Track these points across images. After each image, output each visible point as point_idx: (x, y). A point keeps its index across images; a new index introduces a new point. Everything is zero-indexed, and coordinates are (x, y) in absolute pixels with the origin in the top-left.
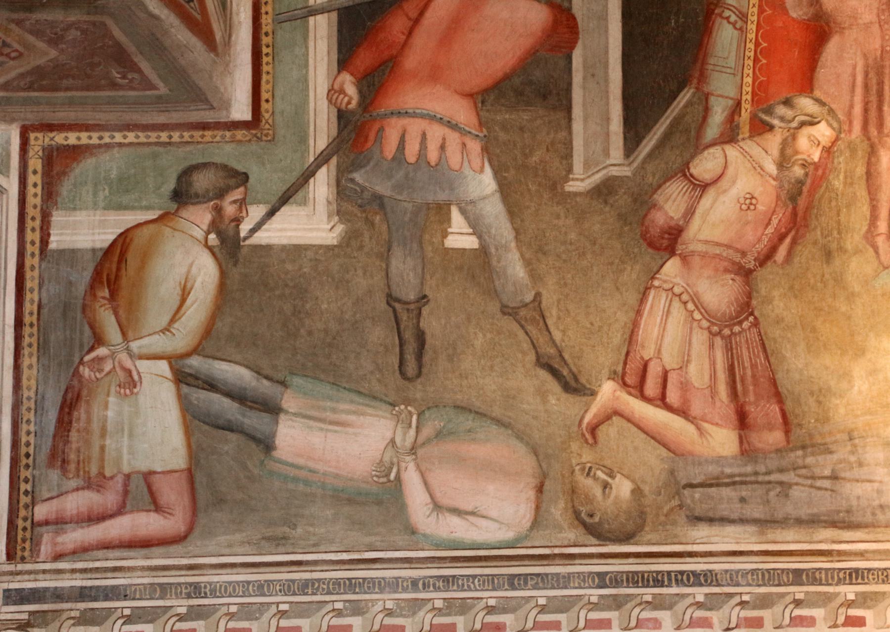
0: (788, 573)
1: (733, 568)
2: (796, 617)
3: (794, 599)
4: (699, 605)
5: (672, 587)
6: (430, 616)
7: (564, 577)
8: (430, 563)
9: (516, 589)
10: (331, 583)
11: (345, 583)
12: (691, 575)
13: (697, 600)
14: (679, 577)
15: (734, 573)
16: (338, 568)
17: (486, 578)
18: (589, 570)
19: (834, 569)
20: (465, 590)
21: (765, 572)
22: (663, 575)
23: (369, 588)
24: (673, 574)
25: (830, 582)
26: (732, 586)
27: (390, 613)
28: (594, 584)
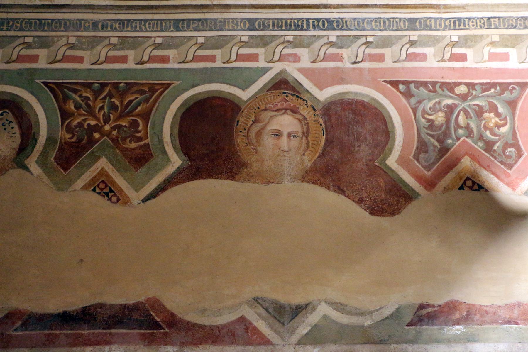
0: (404, 21)
1: (360, 17)
2: (411, 54)
3: (409, 40)
4: (332, 44)
5: (310, 30)
6: (106, 50)
7: (220, 22)
8: (110, 10)
9: (180, 31)
10: (24, 23)
11: (35, 22)
12: (326, 22)
13: (330, 40)
14: (316, 23)
15: (361, 21)
16: (31, 11)
17: (156, 22)
18: (241, 17)
19: (442, 18)
20: (138, 31)
21: (386, 20)
22: (303, 21)
23: (56, 27)
24: (311, 21)
25: (438, 27)
26: (359, 30)
27: (72, 47)
28: (245, 28)
